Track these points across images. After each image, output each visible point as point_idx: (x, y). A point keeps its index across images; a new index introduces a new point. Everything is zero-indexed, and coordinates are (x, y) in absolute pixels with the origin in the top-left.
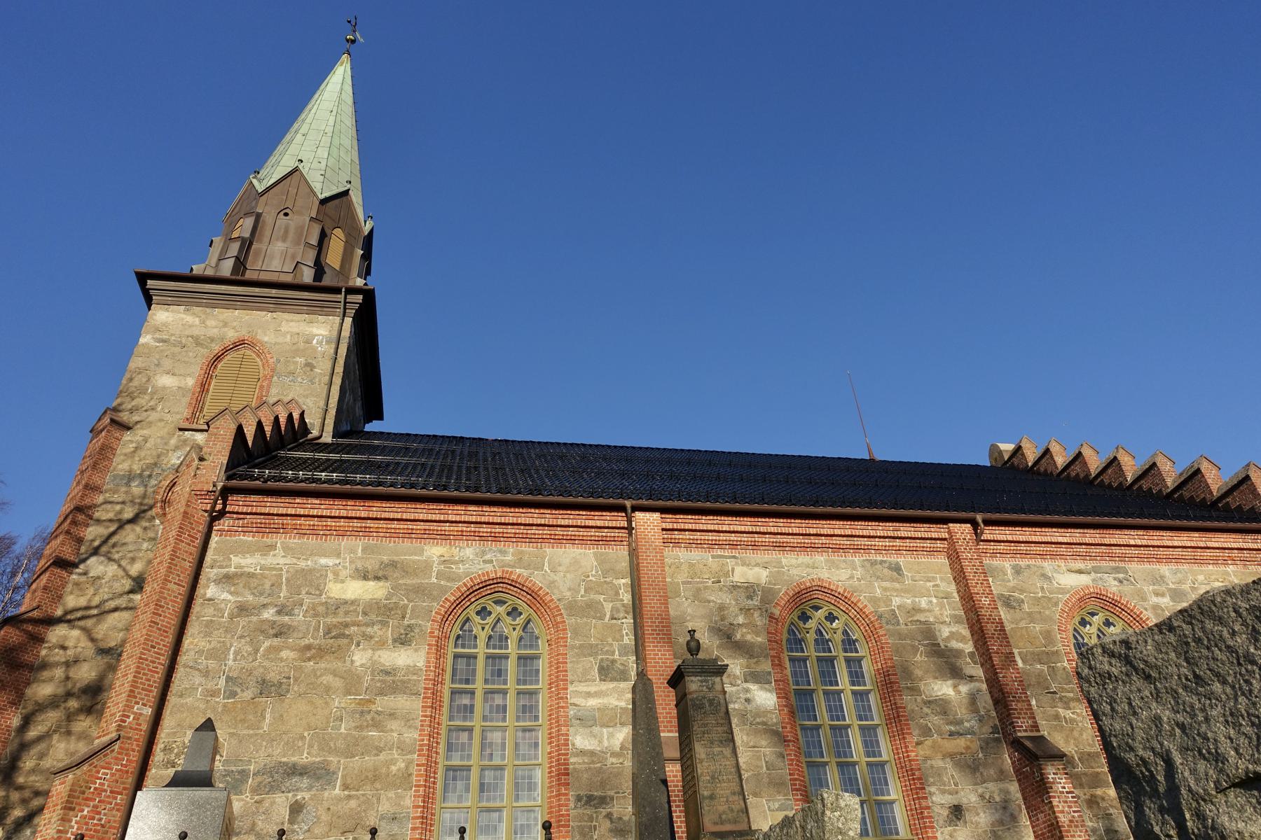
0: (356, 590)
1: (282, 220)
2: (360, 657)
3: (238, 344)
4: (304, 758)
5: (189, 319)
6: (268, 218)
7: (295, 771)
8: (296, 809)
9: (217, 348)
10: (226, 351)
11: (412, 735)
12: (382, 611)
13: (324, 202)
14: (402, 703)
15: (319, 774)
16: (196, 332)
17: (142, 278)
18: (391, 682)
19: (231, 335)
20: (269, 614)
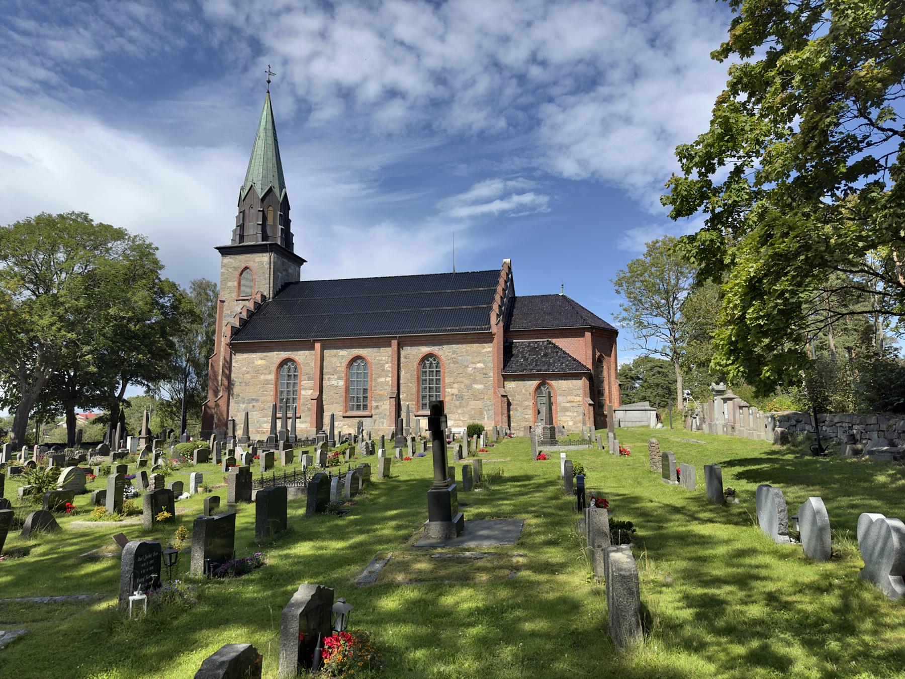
0: (260, 362)
1: (252, 211)
2: (262, 377)
3: (246, 268)
4: (254, 397)
5: (231, 260)
6: (247, 212)
7: (253, 400)
8: (253, 406)
9: (240, 271)
10: (243, 271)
11: (272, 393)
12: (266, 367)
13: (263, 199)
14: (270, 386)
15: (257, 400)
16: (234, 265)
17: (217, 248)
18: (267, 382)
19: (243, 266)
20: (244, 369)
